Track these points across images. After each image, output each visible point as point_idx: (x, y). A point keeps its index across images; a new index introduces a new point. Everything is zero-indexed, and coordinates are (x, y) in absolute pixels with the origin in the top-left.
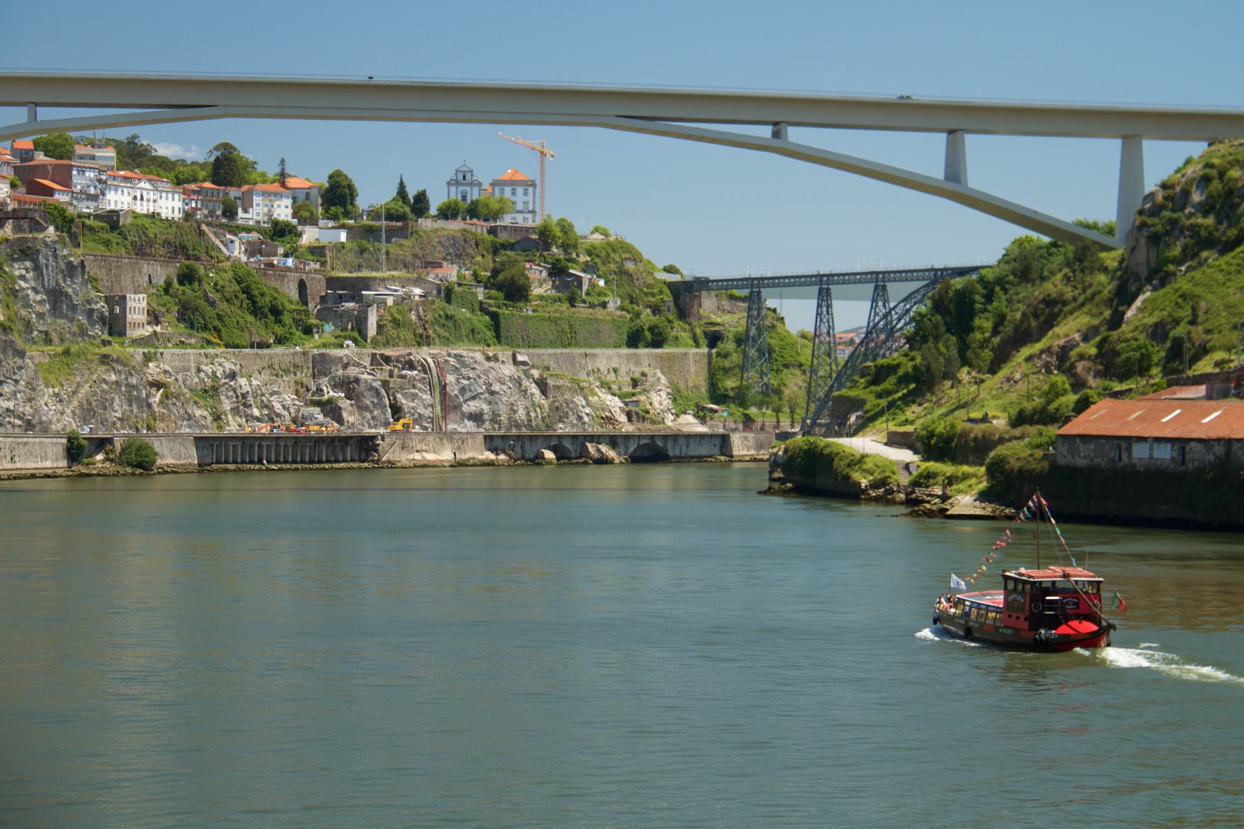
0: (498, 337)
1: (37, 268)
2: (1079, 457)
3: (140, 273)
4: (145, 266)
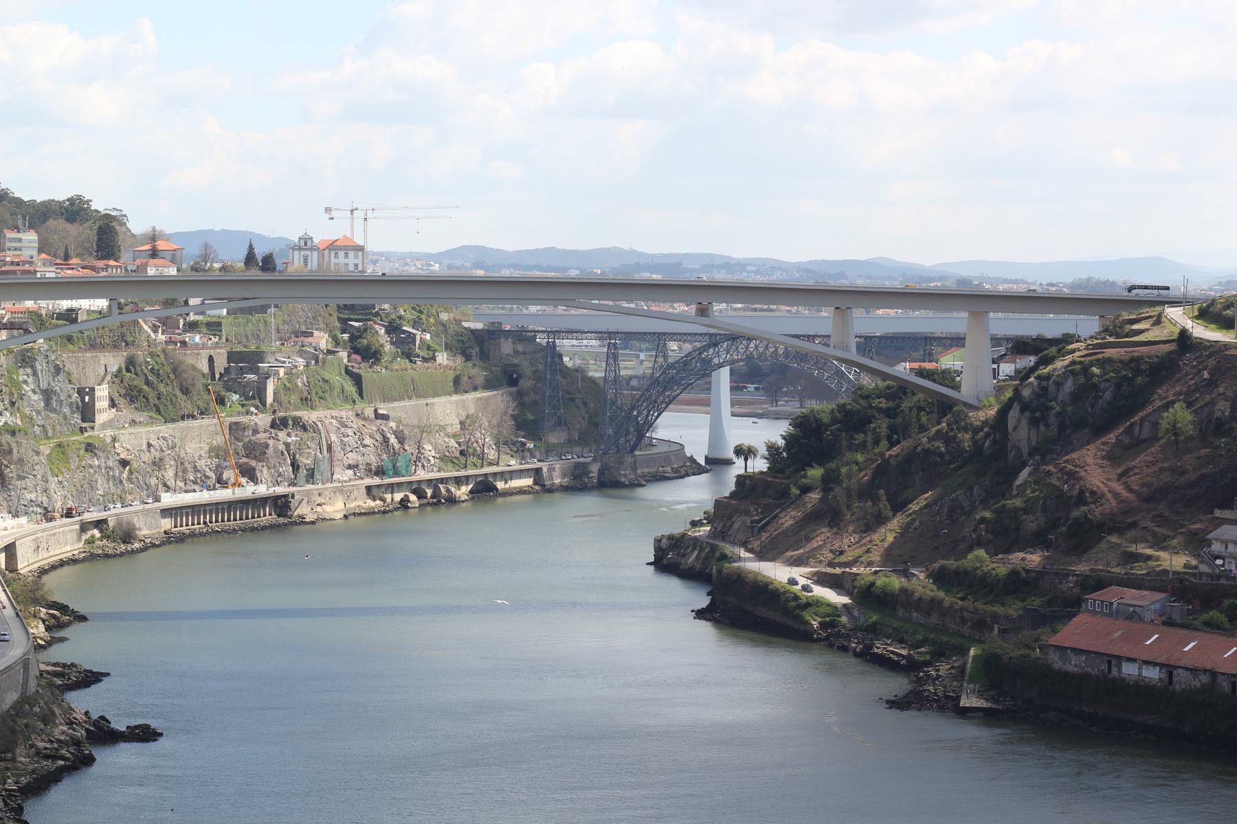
0: (361, 395)
1: (35, 374)
2: (1070, 664)
3: (99, 364)
4: (102, 358)
